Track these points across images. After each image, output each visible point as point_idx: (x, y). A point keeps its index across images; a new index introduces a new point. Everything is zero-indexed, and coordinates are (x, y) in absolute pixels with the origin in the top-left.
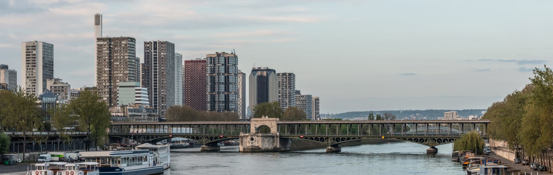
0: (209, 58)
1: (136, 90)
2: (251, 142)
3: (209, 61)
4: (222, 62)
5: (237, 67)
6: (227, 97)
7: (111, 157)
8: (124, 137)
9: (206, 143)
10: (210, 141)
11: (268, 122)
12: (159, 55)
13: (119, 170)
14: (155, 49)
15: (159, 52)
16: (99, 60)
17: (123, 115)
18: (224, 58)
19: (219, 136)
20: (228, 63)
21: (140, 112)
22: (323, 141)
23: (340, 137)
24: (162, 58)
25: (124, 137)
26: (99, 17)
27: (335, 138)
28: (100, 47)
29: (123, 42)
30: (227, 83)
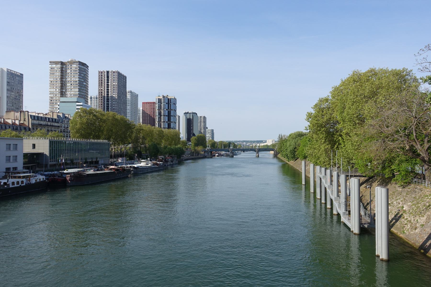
1: (78, 105)
4: (166, 102)
14: (108, 77)
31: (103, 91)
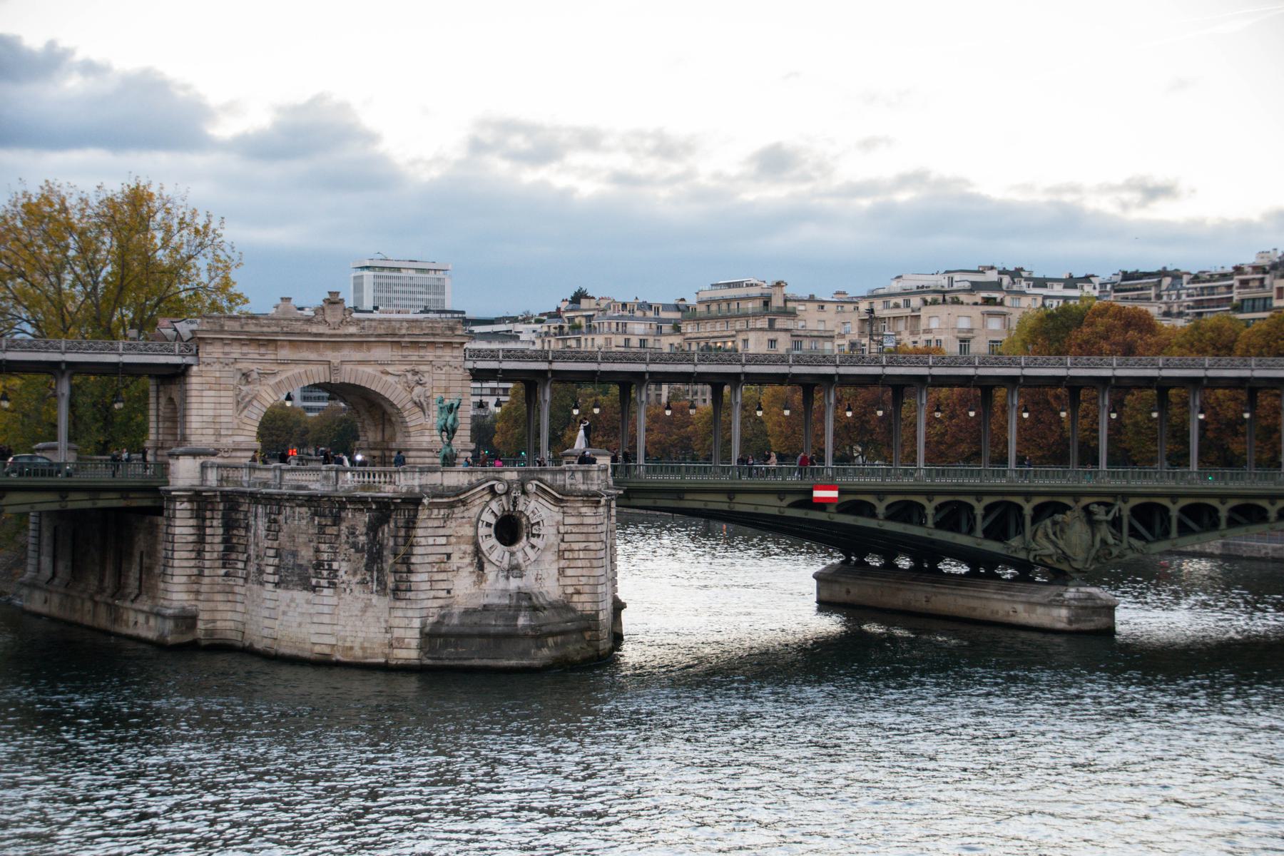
2: (495, 551)
11: (380, 353)
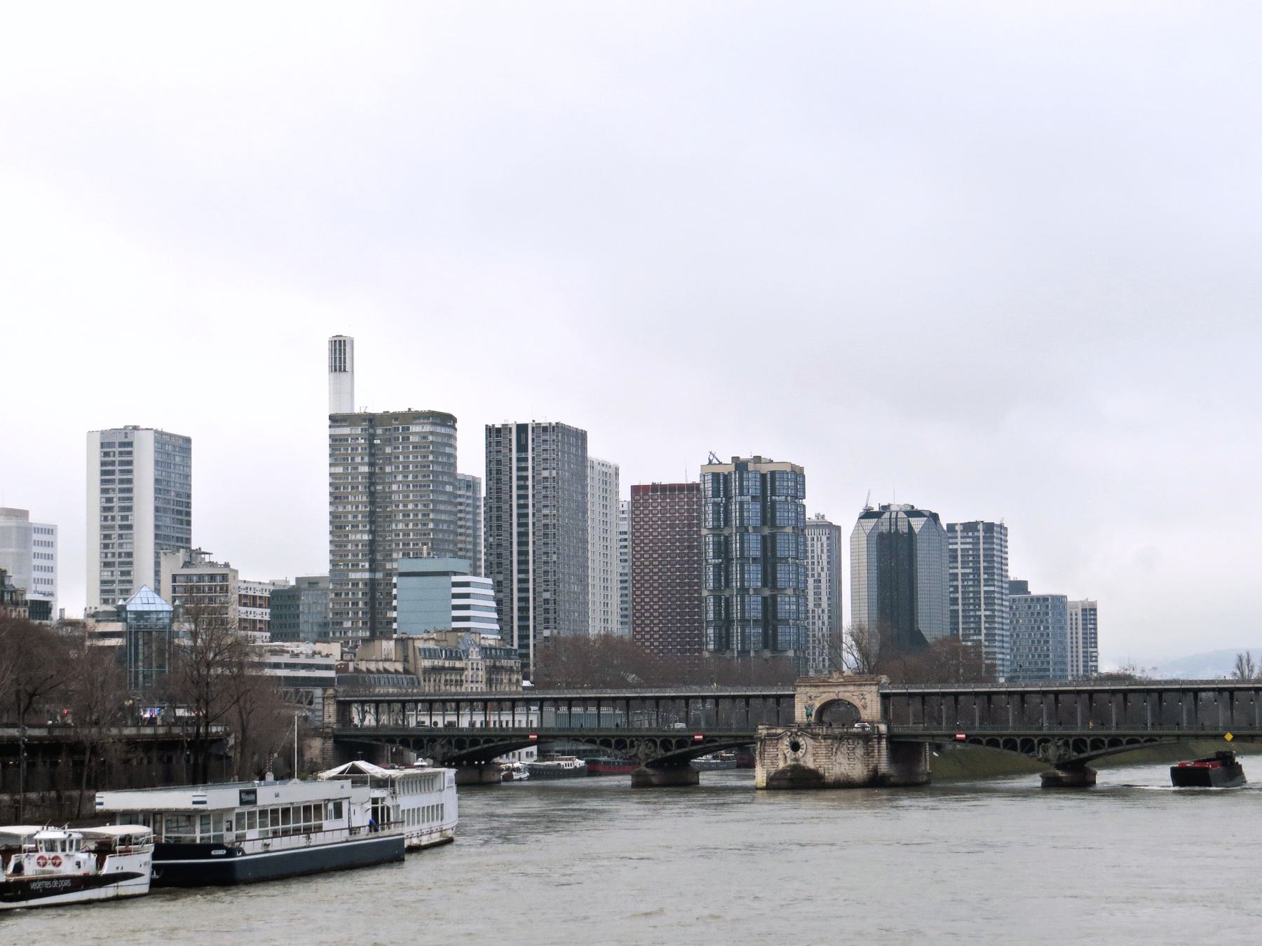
0: (710, 477)
1: (455, 585)
3: (710, 485)
5: (804, 506)
6: (769, 606)
7: (196, 811)
8: (384, 740)
9: (650, 760)
10: (660, 753)
11: (851, 688)
12: (533, 468)
13: (223, 852)
14: (522, 448)
15: (533, 458)
16: (336, 488)
17: (401, 670)
18: (758, 476)
19: (689, 737)
20: (773, 493)
21: (460, 659)
22: (1032, 749)
23: (1086, 738)
24: (545, 478)
25: (384, 740)
26: (345, 345)
27: (1071, 742)
28: (336, 443)
29: (414, 429)
30: (769, 561)
31: (506, 502)
